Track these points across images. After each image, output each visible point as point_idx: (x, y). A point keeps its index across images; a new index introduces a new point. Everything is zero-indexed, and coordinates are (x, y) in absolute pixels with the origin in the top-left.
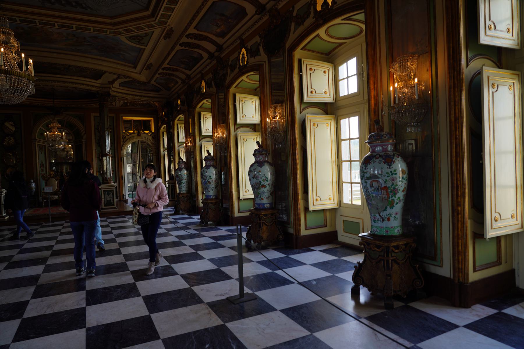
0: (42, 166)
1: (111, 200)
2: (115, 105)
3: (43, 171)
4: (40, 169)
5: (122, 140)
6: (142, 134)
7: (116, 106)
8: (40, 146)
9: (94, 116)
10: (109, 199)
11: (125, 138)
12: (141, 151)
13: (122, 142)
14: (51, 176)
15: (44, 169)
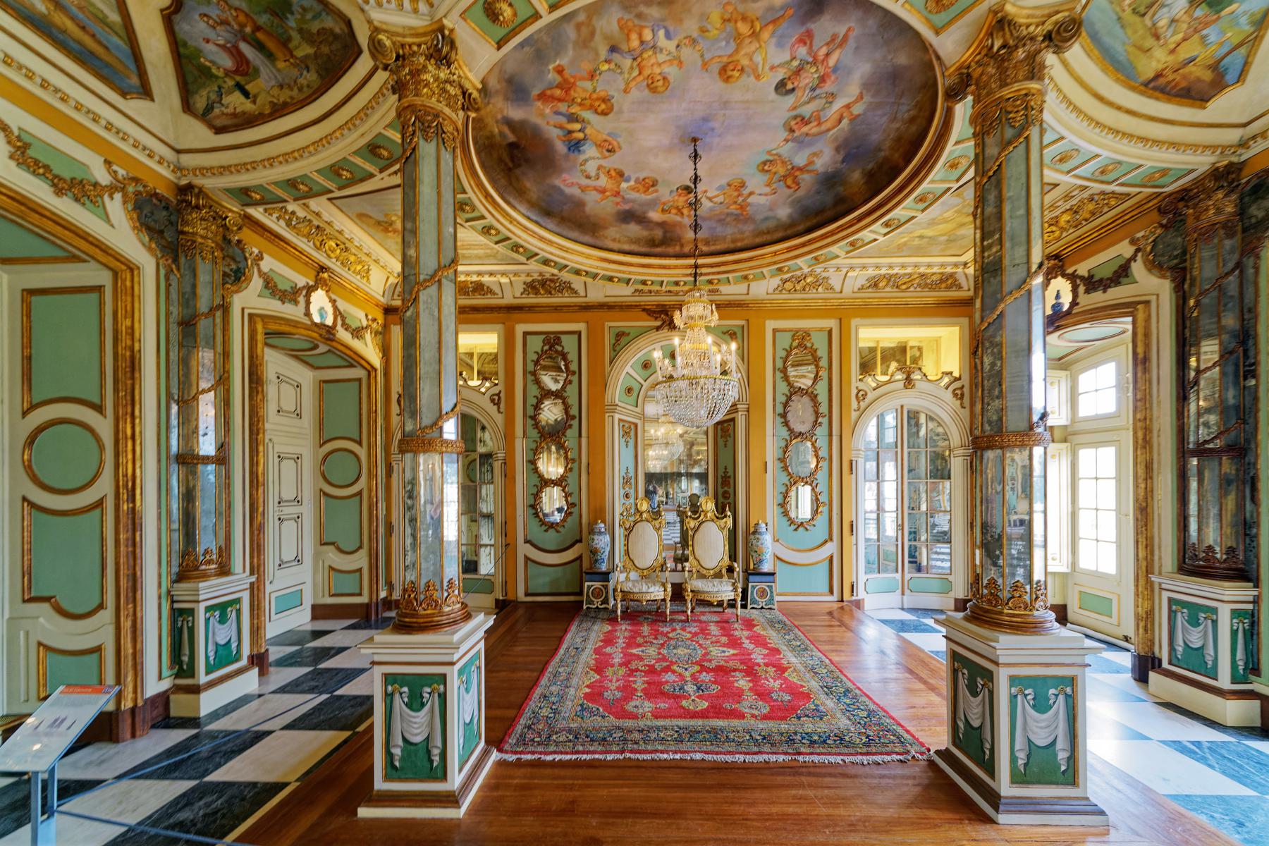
0: (626, 481)
1: (1054, 743)
4: (622, 492)
5: (854, 404)
6: (918, 384)
9: (775, 331)
10: (1041, 740)
11: (865, 396)
12: (909, 442)
15: (632, 492)
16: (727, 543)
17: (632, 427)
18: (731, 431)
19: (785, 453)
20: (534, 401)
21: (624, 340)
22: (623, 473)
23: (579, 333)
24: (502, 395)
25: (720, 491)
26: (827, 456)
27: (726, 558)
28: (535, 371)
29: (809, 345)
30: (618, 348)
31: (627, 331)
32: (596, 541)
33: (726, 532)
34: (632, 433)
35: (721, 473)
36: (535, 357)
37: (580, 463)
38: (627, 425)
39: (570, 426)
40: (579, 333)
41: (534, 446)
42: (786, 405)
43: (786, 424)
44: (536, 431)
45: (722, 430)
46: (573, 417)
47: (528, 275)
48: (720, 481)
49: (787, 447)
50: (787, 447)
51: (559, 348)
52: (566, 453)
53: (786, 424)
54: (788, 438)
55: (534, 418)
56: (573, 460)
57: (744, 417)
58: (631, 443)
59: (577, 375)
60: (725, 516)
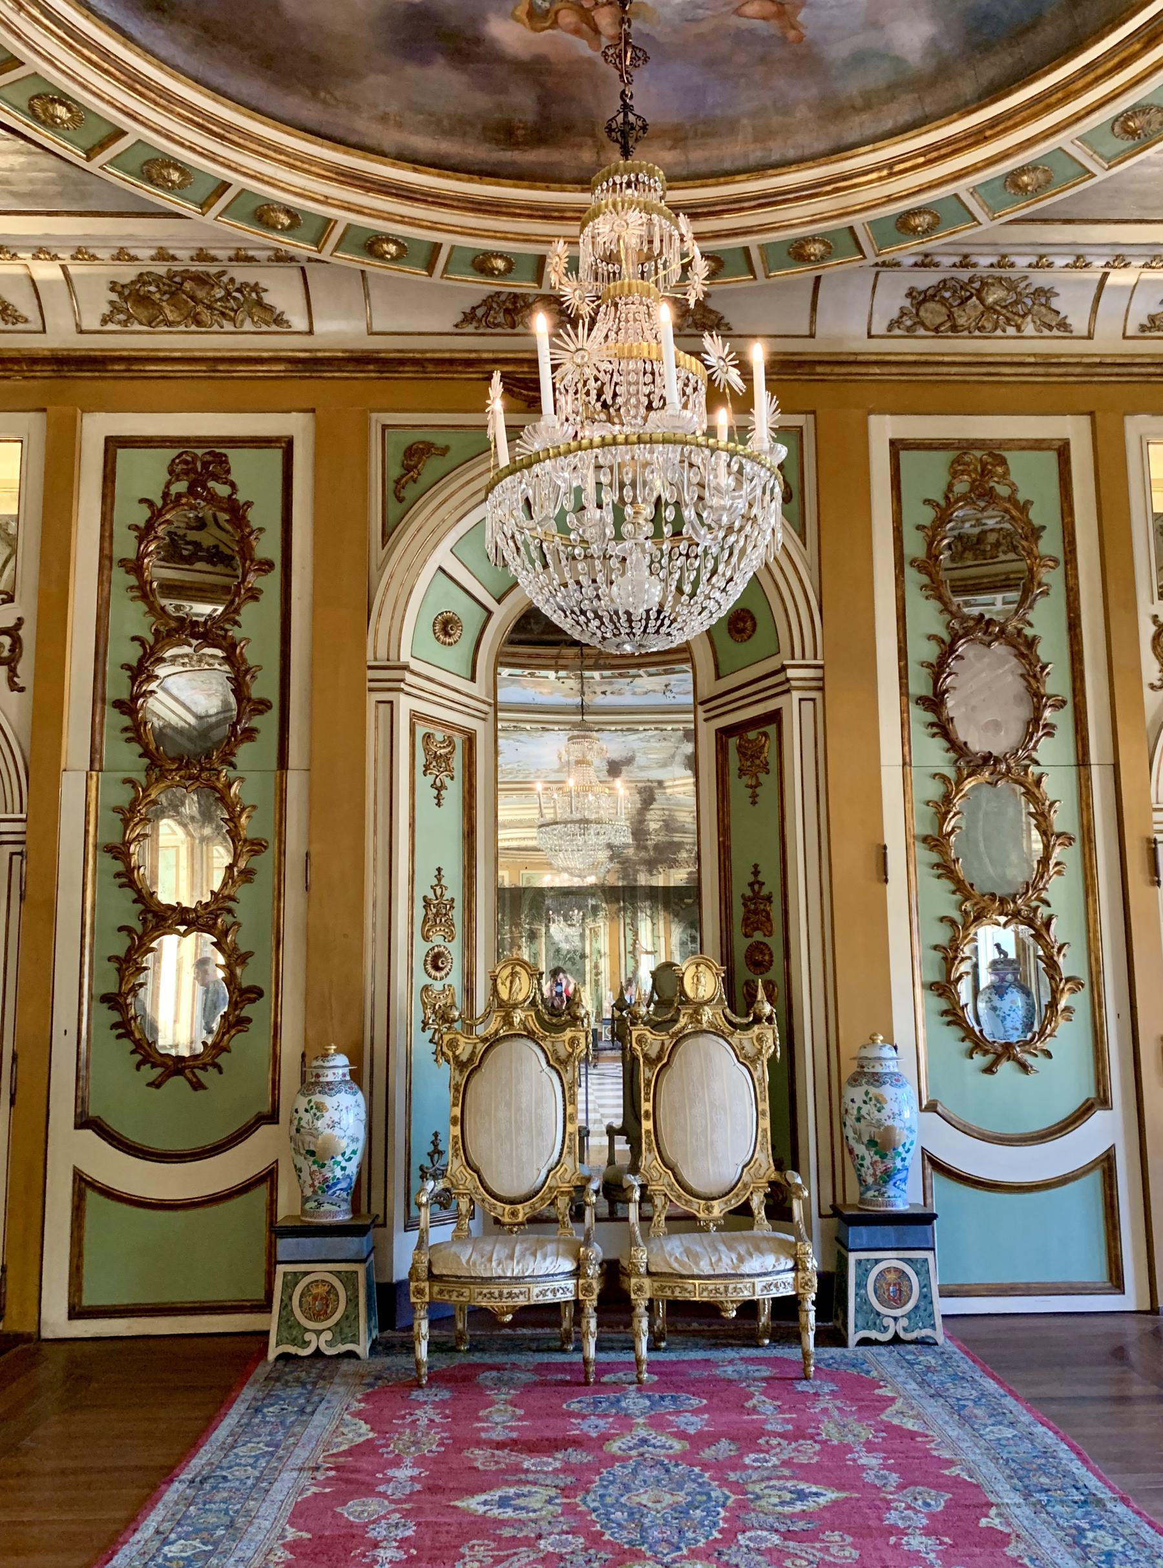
2: (1079, 325)
3: (437, 968)
4: (421, 949)
7: (1090, 337)
8: (428, 737)
9: (897, 446)
13: (1152, 687)
14: (511, 1024)
15: (454, 949)
16: (765, 1106)
17: (458, 739)
18: (770, 753)
19: (943, 817)
20: (132, 653)
21: (431, 467)
22: (424, 889)
23: (287, 446)
24: (27, 634)
25: (741, 944)
26: (1073, 830)
27: (765, 1161)
28: (140, 557)
29: (1002, 490)
30: (409, 493)
31: (440, 440)
32: (330, 1115)
33: (762, 1071)
34: (457, 762)
35: (741, 887)
36: (142, 515)
37: (282, 853)
38: (439, 736)
39: (250, 734)
40: (287, 446)
41: (124, 796)
42: (938, 669)
43: (943, 729)
44: (137, 748)
45: (740, 748)
46: (262, 706)
47: (122, 256)
48: (738, 911)
49: (947, 799)
50: (947, 799)
51: (222, 490)
52: (233, 819)
53: (943, 729)
54: (950, 772)
55: (128, 707)
56: (257, 846)
57: (808, 706)
58: (454, 791)
59: (277, 573)
60: (757, 1020)
